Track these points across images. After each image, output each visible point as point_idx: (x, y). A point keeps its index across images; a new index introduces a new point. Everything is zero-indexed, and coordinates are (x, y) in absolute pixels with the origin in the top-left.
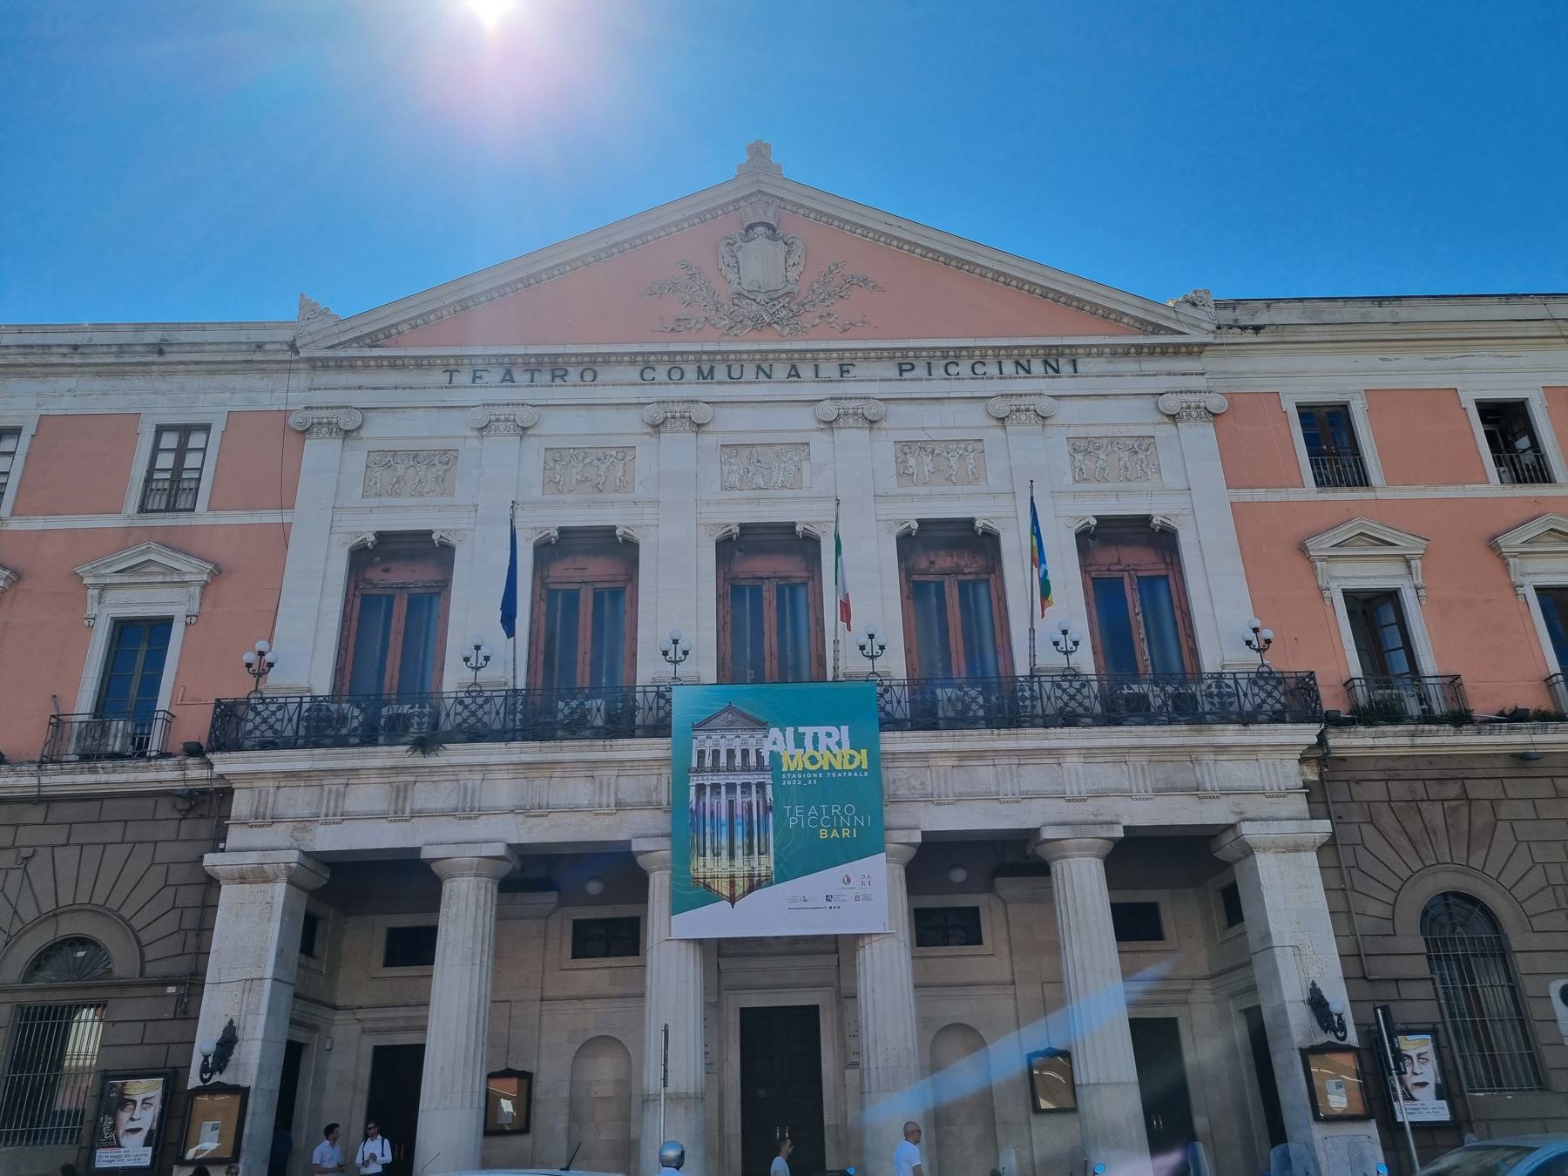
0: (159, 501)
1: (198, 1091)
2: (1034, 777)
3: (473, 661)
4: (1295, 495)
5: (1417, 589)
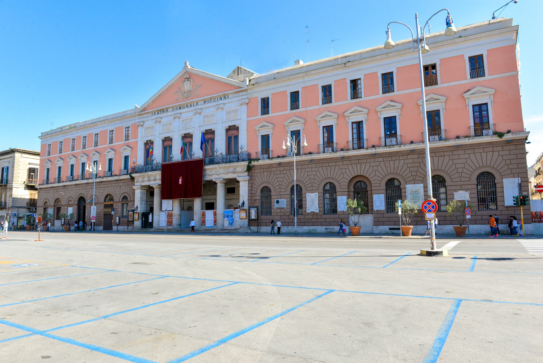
4: (257, 117)
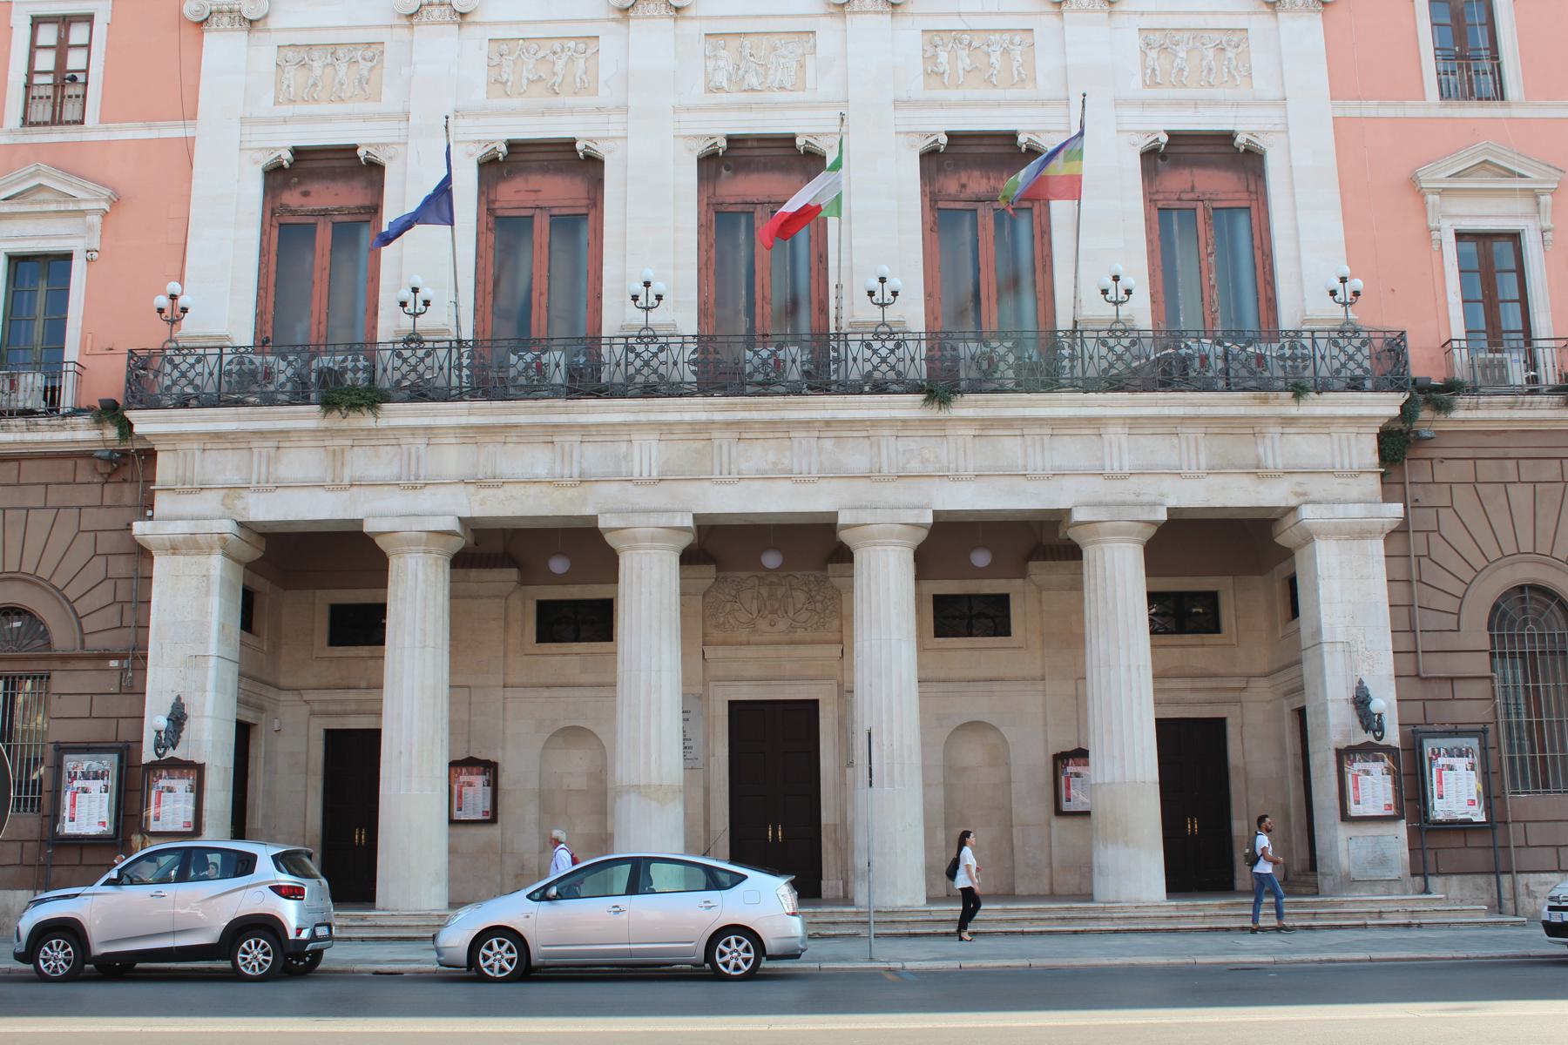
0: (42, 112)
1: (153, 766)
2: (1069, 451)
3: (410, 306)
4: (1413, 110)
5: (1543, 232)
